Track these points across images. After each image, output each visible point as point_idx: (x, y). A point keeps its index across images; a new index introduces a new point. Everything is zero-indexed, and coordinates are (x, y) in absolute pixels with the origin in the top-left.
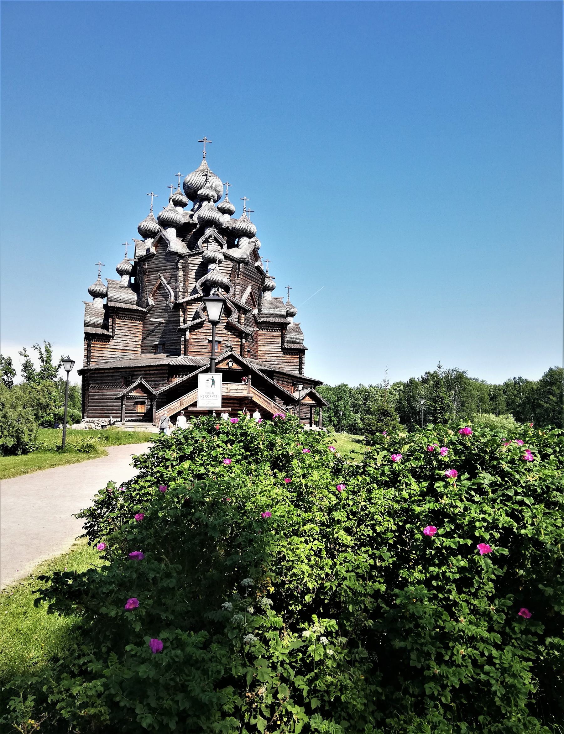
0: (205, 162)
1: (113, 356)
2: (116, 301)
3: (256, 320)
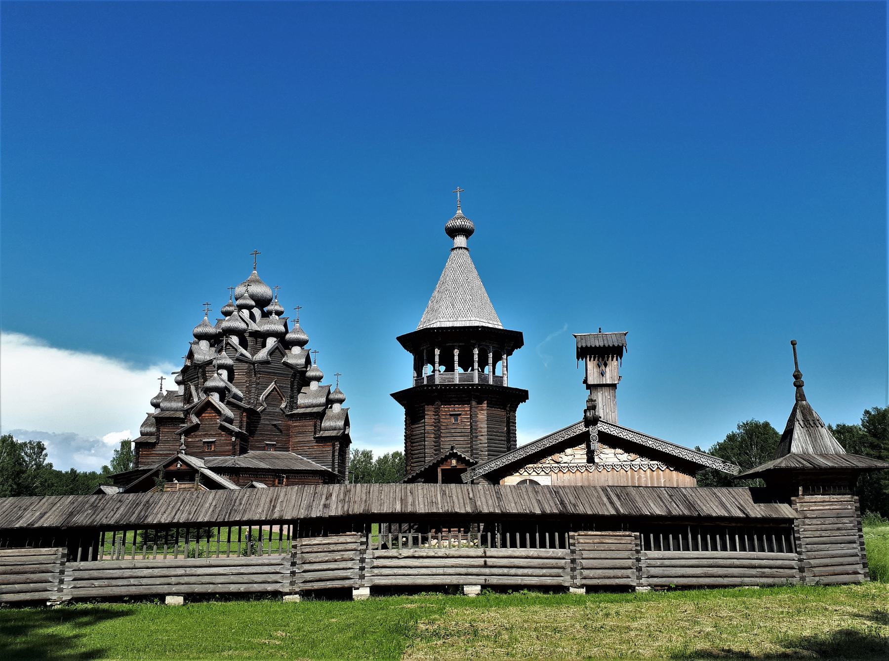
0: (256, 272)
1: (157, 460)
2: (167, 410)
3: (284, 413)
